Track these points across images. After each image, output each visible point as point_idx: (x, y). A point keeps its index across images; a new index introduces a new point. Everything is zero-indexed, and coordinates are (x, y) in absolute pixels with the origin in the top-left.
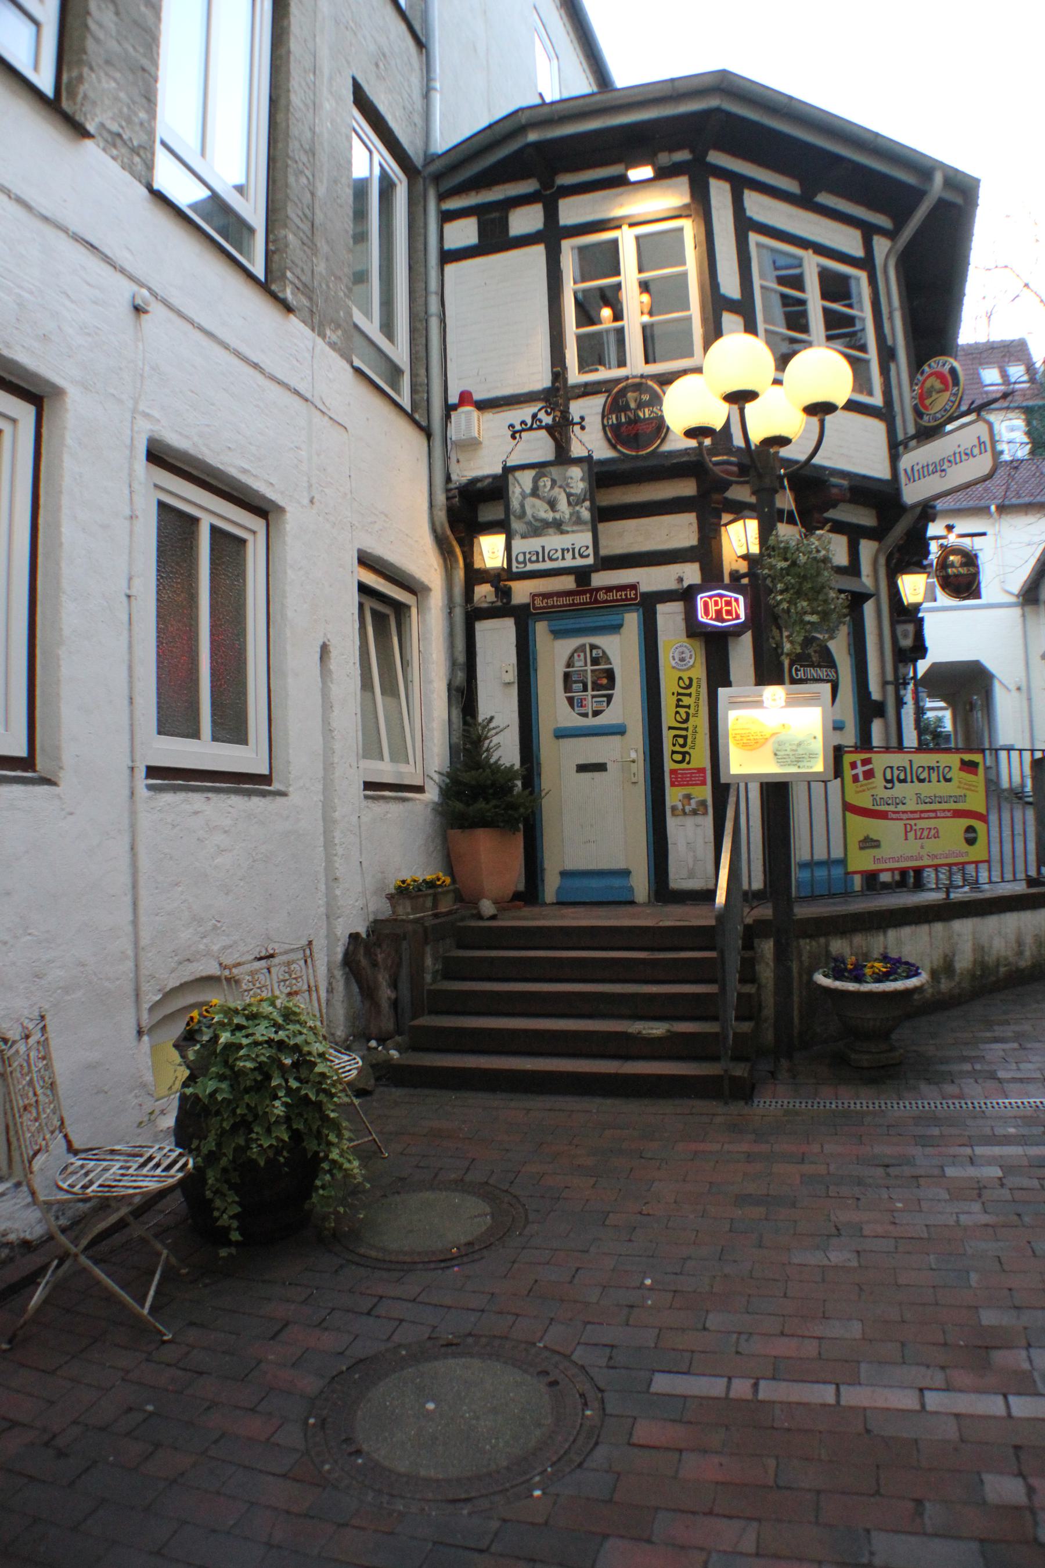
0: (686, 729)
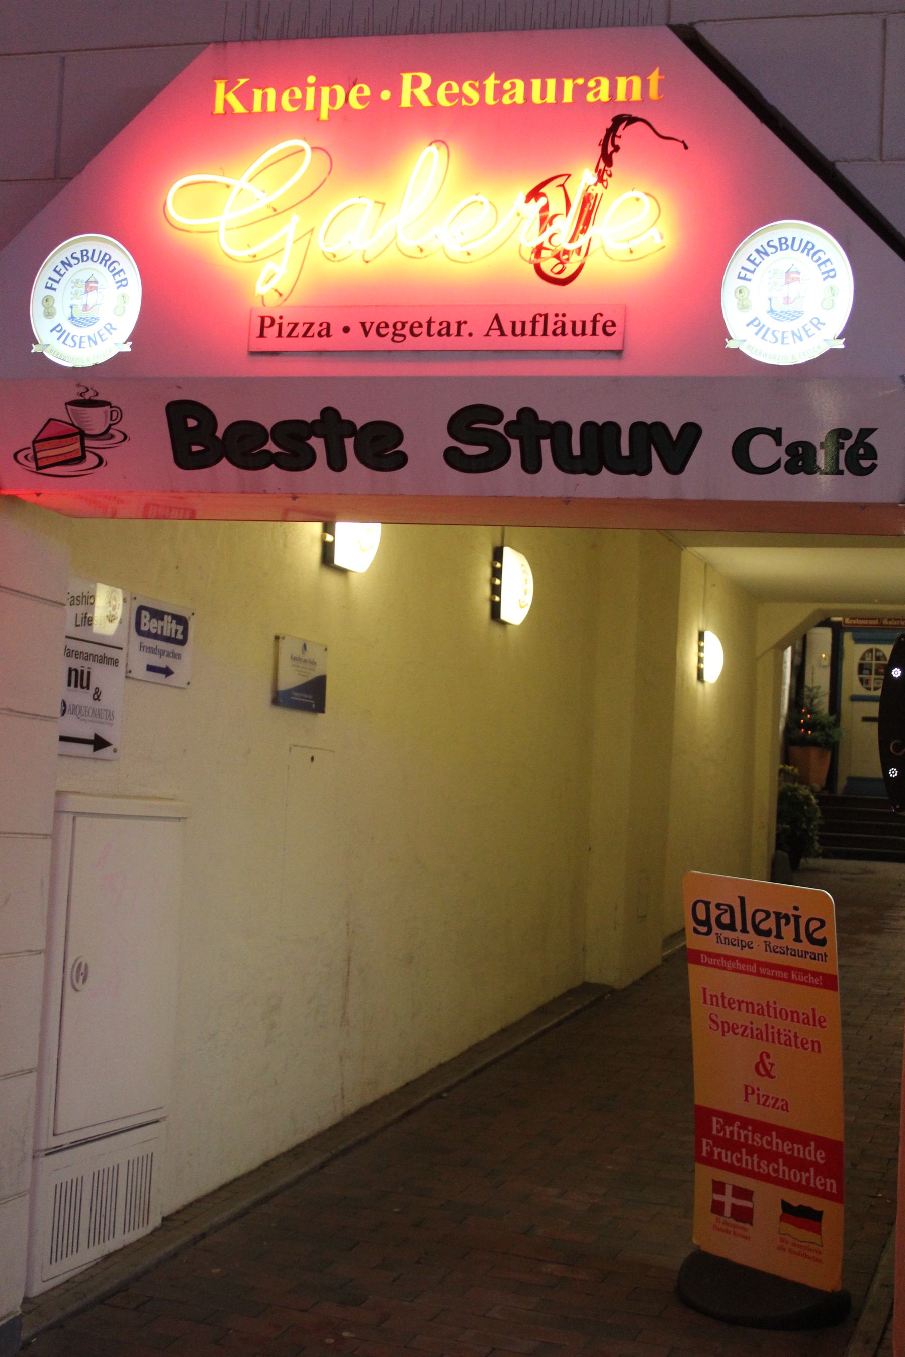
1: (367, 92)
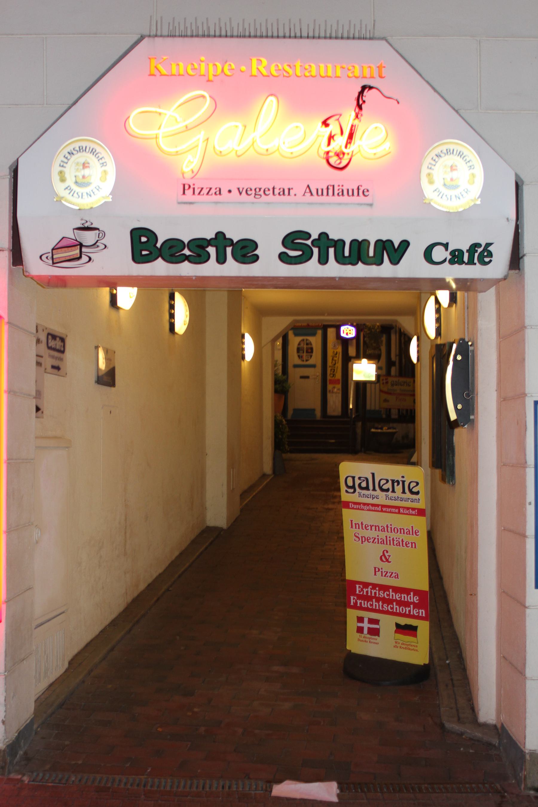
0: (374, 489)
1: (233, 66)
